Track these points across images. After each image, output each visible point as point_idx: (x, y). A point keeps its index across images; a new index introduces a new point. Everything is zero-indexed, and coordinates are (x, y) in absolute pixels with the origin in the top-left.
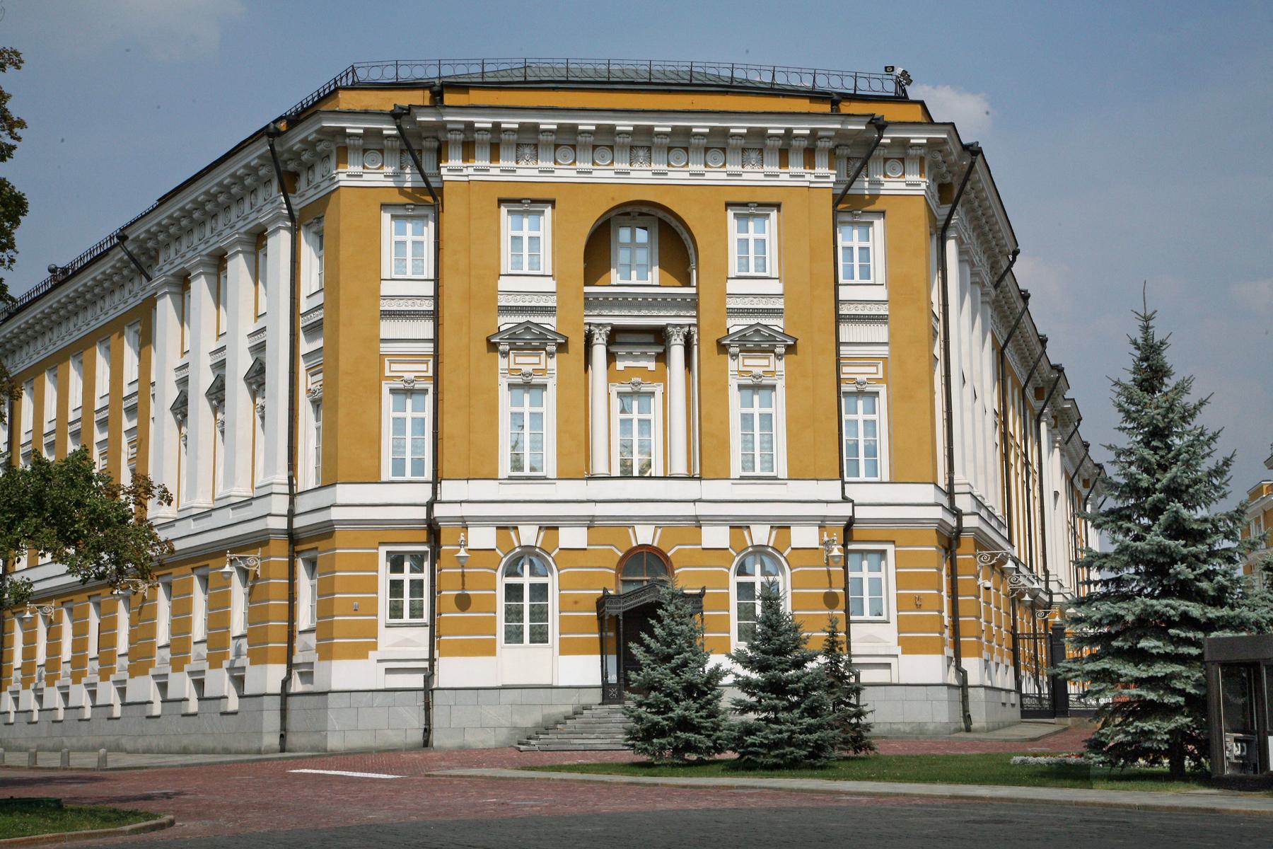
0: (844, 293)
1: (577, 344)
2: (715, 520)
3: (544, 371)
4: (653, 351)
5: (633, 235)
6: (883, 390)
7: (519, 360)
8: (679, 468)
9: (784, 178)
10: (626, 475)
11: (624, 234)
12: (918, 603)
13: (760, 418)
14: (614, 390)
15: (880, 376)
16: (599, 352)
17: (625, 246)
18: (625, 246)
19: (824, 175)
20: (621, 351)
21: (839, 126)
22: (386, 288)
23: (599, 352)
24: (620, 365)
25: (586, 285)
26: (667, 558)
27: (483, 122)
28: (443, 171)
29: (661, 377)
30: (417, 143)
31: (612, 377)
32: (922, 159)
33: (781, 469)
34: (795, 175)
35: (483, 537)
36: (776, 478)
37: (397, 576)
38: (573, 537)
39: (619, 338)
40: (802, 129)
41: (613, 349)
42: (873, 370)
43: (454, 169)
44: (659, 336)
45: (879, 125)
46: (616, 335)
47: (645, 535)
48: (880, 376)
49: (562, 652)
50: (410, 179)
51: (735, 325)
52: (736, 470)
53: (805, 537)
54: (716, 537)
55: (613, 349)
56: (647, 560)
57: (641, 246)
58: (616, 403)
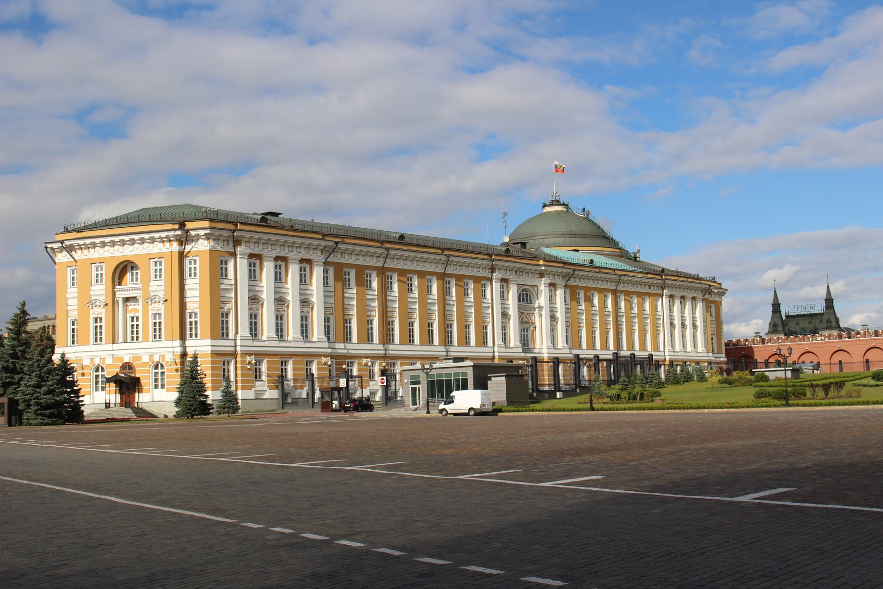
2: (143, 354)
6: (198, 311)
9: (164, 250)
19: (175, 247)
22: (69, 290)
24: (130, 308)
35: (86, 362)
38: (109, 361)
40: (163, 235)
43: (78, 255)
44: (134, 299)
45: (188, 231)
46: (127, 300)
47: (126, 360)
51: (152, 294)
54: (145, 359)
56: (128, 366)
58: (129, 320)
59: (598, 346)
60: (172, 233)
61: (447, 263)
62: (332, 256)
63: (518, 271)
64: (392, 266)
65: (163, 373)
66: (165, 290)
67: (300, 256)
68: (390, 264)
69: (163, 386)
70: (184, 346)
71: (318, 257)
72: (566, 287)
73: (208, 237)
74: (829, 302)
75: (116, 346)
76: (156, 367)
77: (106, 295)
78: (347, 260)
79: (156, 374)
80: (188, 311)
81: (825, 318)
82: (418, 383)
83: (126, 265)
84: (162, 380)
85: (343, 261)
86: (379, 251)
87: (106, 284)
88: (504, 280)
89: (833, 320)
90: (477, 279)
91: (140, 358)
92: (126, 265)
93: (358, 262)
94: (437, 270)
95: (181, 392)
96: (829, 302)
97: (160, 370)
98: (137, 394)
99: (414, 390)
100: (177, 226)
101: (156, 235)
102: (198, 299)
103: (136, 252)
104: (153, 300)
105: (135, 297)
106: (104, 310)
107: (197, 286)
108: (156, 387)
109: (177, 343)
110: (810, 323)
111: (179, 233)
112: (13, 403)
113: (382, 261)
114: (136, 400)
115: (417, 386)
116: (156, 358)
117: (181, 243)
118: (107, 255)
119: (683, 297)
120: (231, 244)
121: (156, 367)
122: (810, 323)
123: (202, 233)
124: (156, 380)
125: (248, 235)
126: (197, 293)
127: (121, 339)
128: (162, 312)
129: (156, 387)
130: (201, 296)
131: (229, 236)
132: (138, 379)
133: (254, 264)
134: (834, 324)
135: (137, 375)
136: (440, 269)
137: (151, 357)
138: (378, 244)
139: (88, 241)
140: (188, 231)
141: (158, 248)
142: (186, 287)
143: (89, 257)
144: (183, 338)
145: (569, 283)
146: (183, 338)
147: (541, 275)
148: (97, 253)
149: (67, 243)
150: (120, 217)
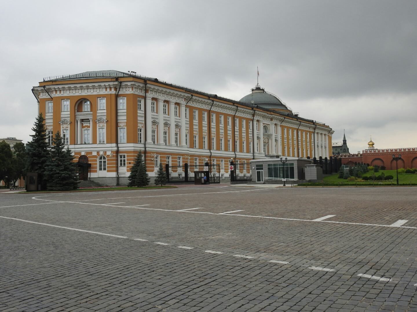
0: (119, 111)
1: (73, 122)
2: (94, 151)
3: (68, 127)
4: (89, 123)
5: (87, 103)
6: (126, 127)
7: (64, 126)
8: (91, 142)
9: (106, 93)
10: (85, 144)
11: (86, 103)
12: (130, 163)
13: (102, 132)
14: (83, 129)
15: (125, 125)
16: (79, 123)
17: (86, 105)
18: (86, 105)
19: (113, 92)
20: (83, 123)
21: (113, 83)
23: (79, 123)
25: (78, 112)
26: (87, 157)
27: (56, 87)
28: (53, 95)
29: (89, 127)
30: (48, 91)
31: (83, 127)
32: (132, 88)
33: (105, 142)
34: (108, 92)
36: (104, 143)
37: (121, 159)
39: (84, 121)
40: (107, 84)
41: (82, 123)
42: (124, 124)
43: (54, 95)
44: (88, 120)
46: (82, 120)
48: (125, 125)
49: (107, 172)
50: (49, 97)
51: (98, 118)
52: (98, 142)
53: (109, 153)
54: (95, 154)
55: (82, 123)
57: (88, 105)
59: (286, 155)
60: (111, 83)
61: (237, 110)
62: (188, 103)
63: (264, 117)
64: (213, 110)
65: (105, 162)
66: (107, 116)
67: (175, 101)
68: (214, 109)
69: (105, 169)
70: (118, 147)
71: (183, 102)
72: (281, 126)
73: (132, 87)
74: (345, 141)
75: (77, 146)
76: (101, 158)
77: (70, 117)
78: (195, 105)
79: (100, 162)
80: (119, 128)
81: (343, 148)
82: (262, 169)
83: (82, 101)
84: (105, 165)
85: (193, 105)
86: (209, 101)
87: (70, 111)
88: (258, 121)
89: (346, 149)
90: (248, 120)
91: (91, 153)
92: (82, 101)
93: (199, 107)
94: (232, 114)
95: (132, 172)
96: (345, 141)
97: (103, 160)
98: (89, 173)
99: (259, 173)
100: (114, 80)
101: (103, 84)
102: (126, 121)
103: (89, 94)
104: (100, 121)
105: (88, 119)
106: (69, 126)
107: (126, 114)
108: (100, 169)
109: (114, 145)
110: (336, 150)
111: (116, 83)
112: (40, 176)
113: (210, 107)
114: (89, 177)
115: (261, 171)
116: (101, 153)
117: (116, 89)
118: (71, 94)
119: (321, 134)
120: (143, 92)
121: (101, 158)
122: (336, 150)
123: (129, 84)
124: (100, 166)
125: (152, 87)
126: (125, 118)
127: (79, 143)
128: (105, 128)
129: (100, 169)
130: (127, 119)
131: (143, 87)
132: (90, 164)
133: (154, 103)
134: (347, 151)
135: (89, 163)
136: (232, 113)
137: (98, 152)
138: (207, 98)
139: (60, 87)
140: (121, 83)
141: (103, 92)
142: (119, 114)
143: (60, 95)
144: (117, 143)
145: (282, 124)
146: (117, 143)
147: (271, 119)
148: (67, 94)
149: (47, 87)
150: (78, 75)
